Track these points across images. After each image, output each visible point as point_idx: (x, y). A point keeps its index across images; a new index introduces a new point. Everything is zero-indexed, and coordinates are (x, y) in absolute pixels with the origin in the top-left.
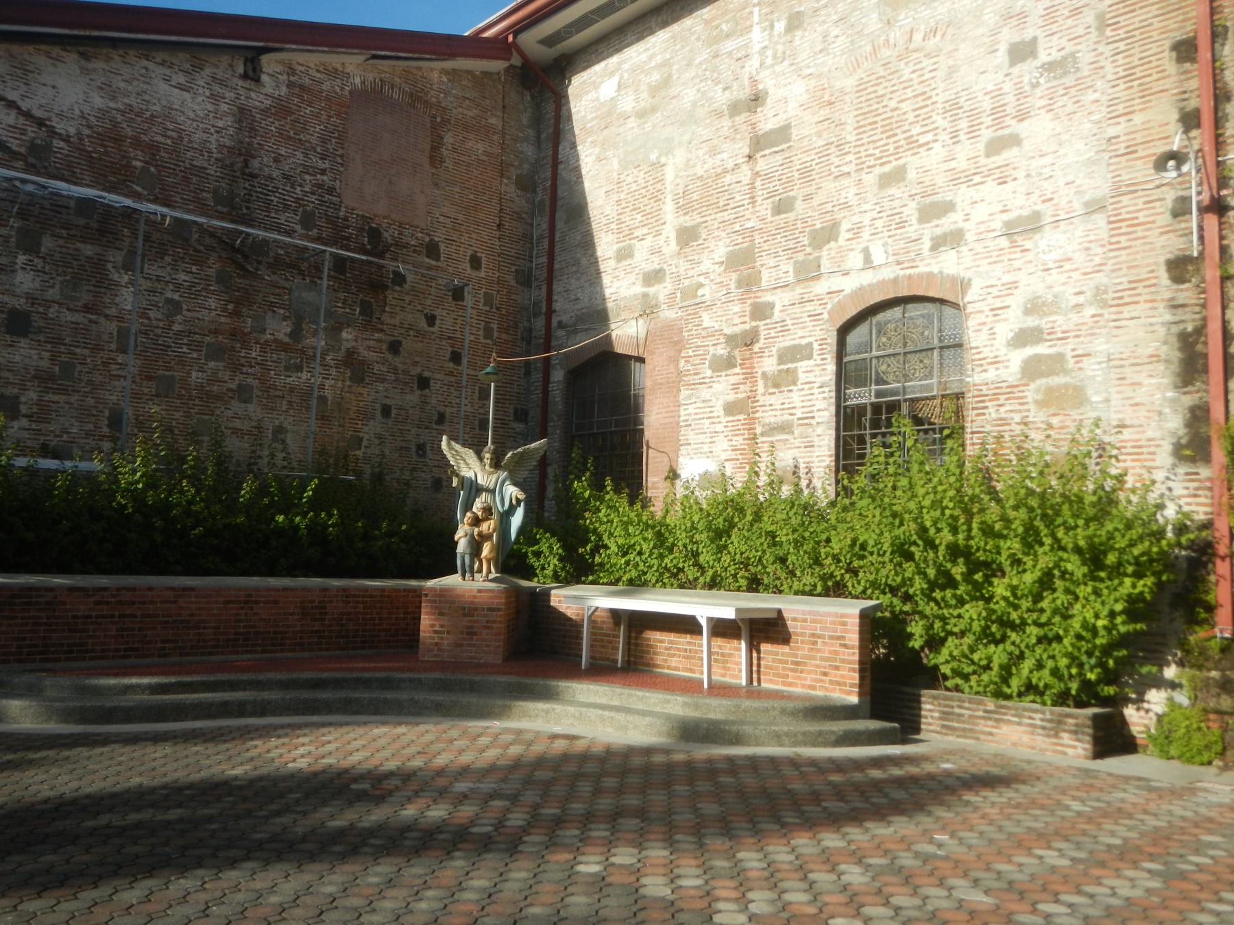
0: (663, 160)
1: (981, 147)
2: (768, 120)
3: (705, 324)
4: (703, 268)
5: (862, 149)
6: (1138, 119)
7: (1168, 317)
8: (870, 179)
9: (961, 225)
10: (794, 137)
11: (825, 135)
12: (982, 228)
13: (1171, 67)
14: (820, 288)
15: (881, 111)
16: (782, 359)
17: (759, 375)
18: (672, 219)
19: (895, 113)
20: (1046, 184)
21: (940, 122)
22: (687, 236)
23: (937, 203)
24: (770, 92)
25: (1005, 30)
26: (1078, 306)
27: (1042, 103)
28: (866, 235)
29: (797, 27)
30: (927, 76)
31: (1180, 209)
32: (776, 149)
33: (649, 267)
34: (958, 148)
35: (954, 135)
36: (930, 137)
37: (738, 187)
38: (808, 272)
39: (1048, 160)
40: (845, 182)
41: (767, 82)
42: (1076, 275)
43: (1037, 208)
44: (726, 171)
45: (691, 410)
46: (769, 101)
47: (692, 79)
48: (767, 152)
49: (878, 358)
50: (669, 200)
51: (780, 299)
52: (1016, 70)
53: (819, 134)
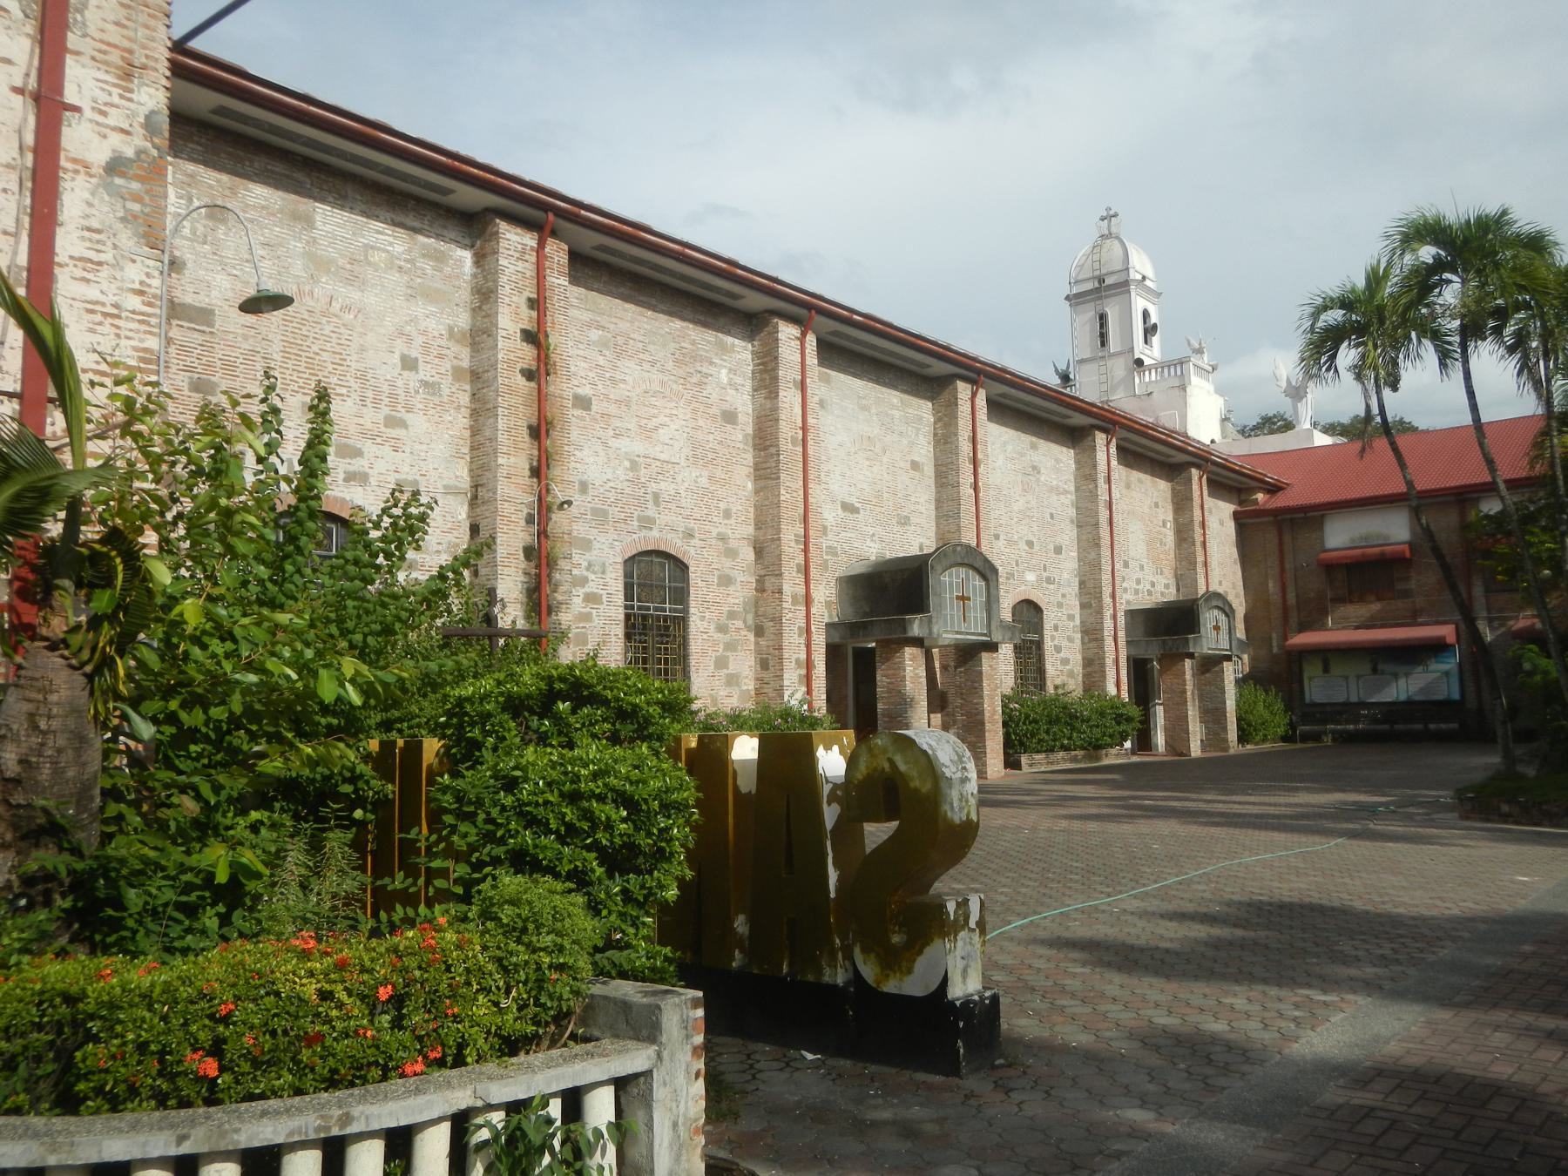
1: (380, 418)
5: (288, 372)
6: (513, 459)
7: (522, 579)
9: (368, 470)
10: (217, 326)
11: (251, 341)
12: (382, 478)
13: (527, 439)
15: (305, 348)
19: (317, 357)
20: (422, 463)
21: (352, 383)
23: (348, 446)
24: (189, 265)
25: (399, 341)
26: (438, 551)
27: (420, 406)
30: (343, 342)
31: (529, 520)
32: (193, 325)
34: (365, 410)
36: (344, 391)
39: (424, 447)
42: (438, 531)
43: (418, 477)
46: (186, 272)
48: (186, 324)
52: (406, 373)
53: (245, 337)
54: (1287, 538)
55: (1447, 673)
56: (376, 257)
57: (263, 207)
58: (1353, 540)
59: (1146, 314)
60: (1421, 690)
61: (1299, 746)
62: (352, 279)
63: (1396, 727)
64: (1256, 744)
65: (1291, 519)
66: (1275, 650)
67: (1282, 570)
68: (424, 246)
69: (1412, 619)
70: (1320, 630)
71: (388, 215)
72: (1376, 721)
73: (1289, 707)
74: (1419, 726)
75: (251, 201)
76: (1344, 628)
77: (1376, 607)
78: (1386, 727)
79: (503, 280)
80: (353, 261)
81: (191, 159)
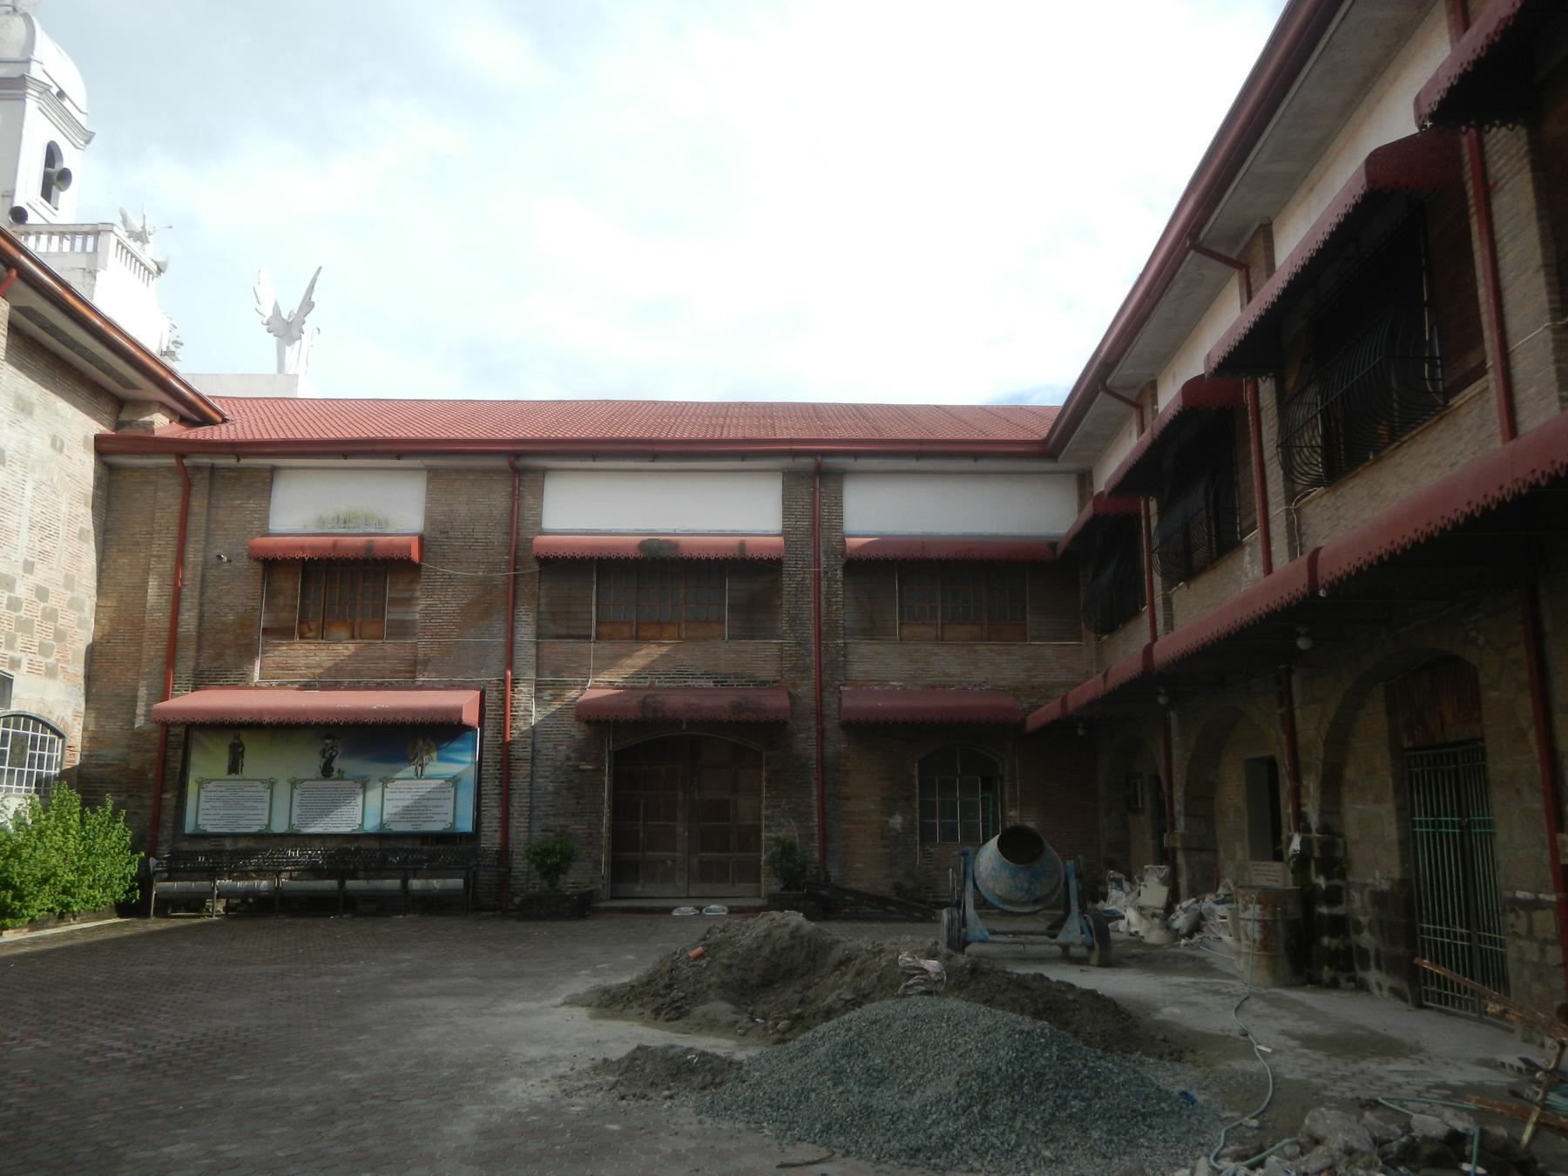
54: (198, 504)
55: (455, 781)
58: (321, 521)
59: (52, 154)
60: (407, 811)
61: (154, 924)
63: (351, 884)
64: (34, 924)
65: (213, 469)
66: (140, 722)
67: (180, 561)
69: (408, 677)
70: (234, 686)
72: (315, 871)
73: (143, 842)
74: (392, 884)
76: (281, 686)
77: (345, 649)
78: (330, 884)
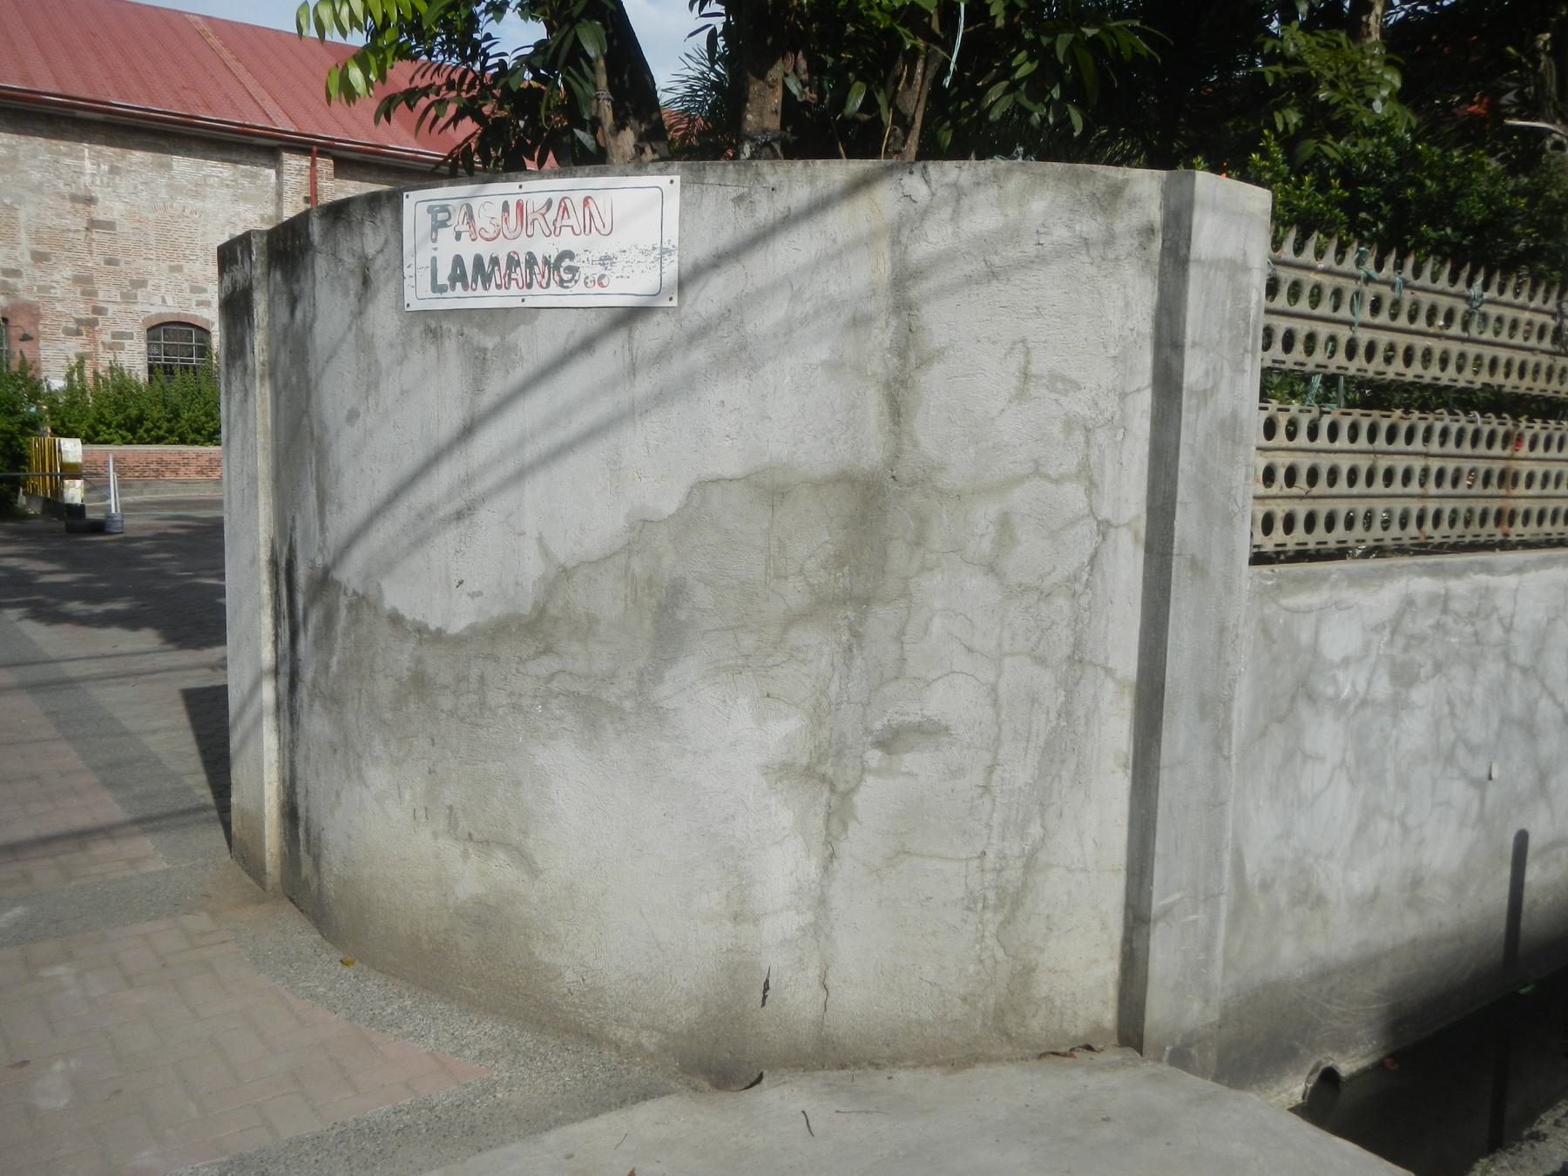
0: (16, 206)
2: (99, 213)
3: (58, 309)
4: (54, 278)
8: (165, 265)
14: (137, 308)
16: (114, 336)
17: (99, 342)
18: (25, 245)
22: (39, 257)
24: (100, 200)
28: (163, 290)
29: (117, 174)
33: (6, 266)
35: (206, 261)
37: (79, 242)
38: (128, 298)
40: (150, 262)
41: (97, 192)
44: (69, 230)
45: (48, 353)
47: (38, 167)
49: (165, 345)
50: (22, 231)
51: (111, 308)
56: (211, 181)
57: (142, 163)
62: (196, 195)
68: (243, 171)
71: (219, 156)
75: (134, 160)
79: (286, 188)
80: (197, 185)
81: (98, 143)
